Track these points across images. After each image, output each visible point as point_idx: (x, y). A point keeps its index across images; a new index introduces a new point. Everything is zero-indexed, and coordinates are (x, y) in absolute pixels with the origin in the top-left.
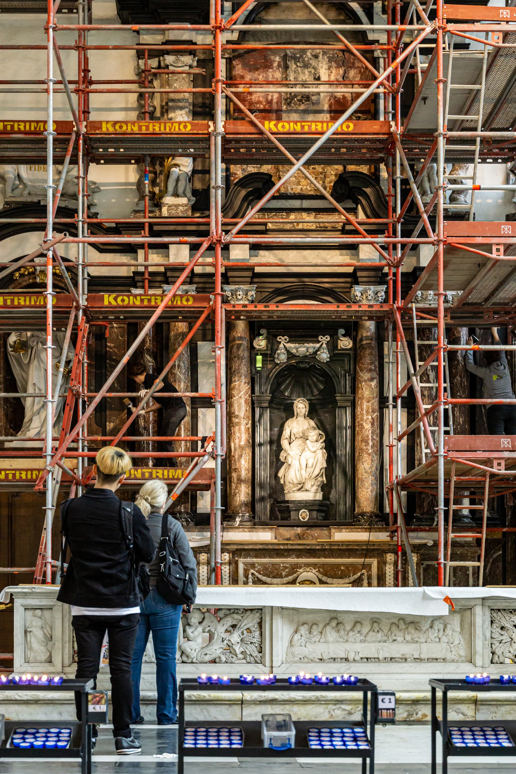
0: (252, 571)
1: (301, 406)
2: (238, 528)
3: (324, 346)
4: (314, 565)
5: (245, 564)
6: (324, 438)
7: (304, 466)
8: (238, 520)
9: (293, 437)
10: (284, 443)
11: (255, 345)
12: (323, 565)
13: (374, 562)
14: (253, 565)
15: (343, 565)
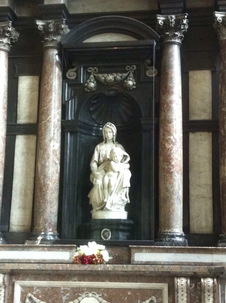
0: (29, 295)
1: (111, 130)
2: (38, 247)
3: (131, 75)
4: (97, 290)
5: (23, 287)
6: (129, 159)
7: (106, 186)
8: (40, 238)
9: (101, 159)
10: (94, 165)
11: (67, 76)
12: (107, 290)
13: (164, 287)
14: (31, 289)
15: (130, 289)
